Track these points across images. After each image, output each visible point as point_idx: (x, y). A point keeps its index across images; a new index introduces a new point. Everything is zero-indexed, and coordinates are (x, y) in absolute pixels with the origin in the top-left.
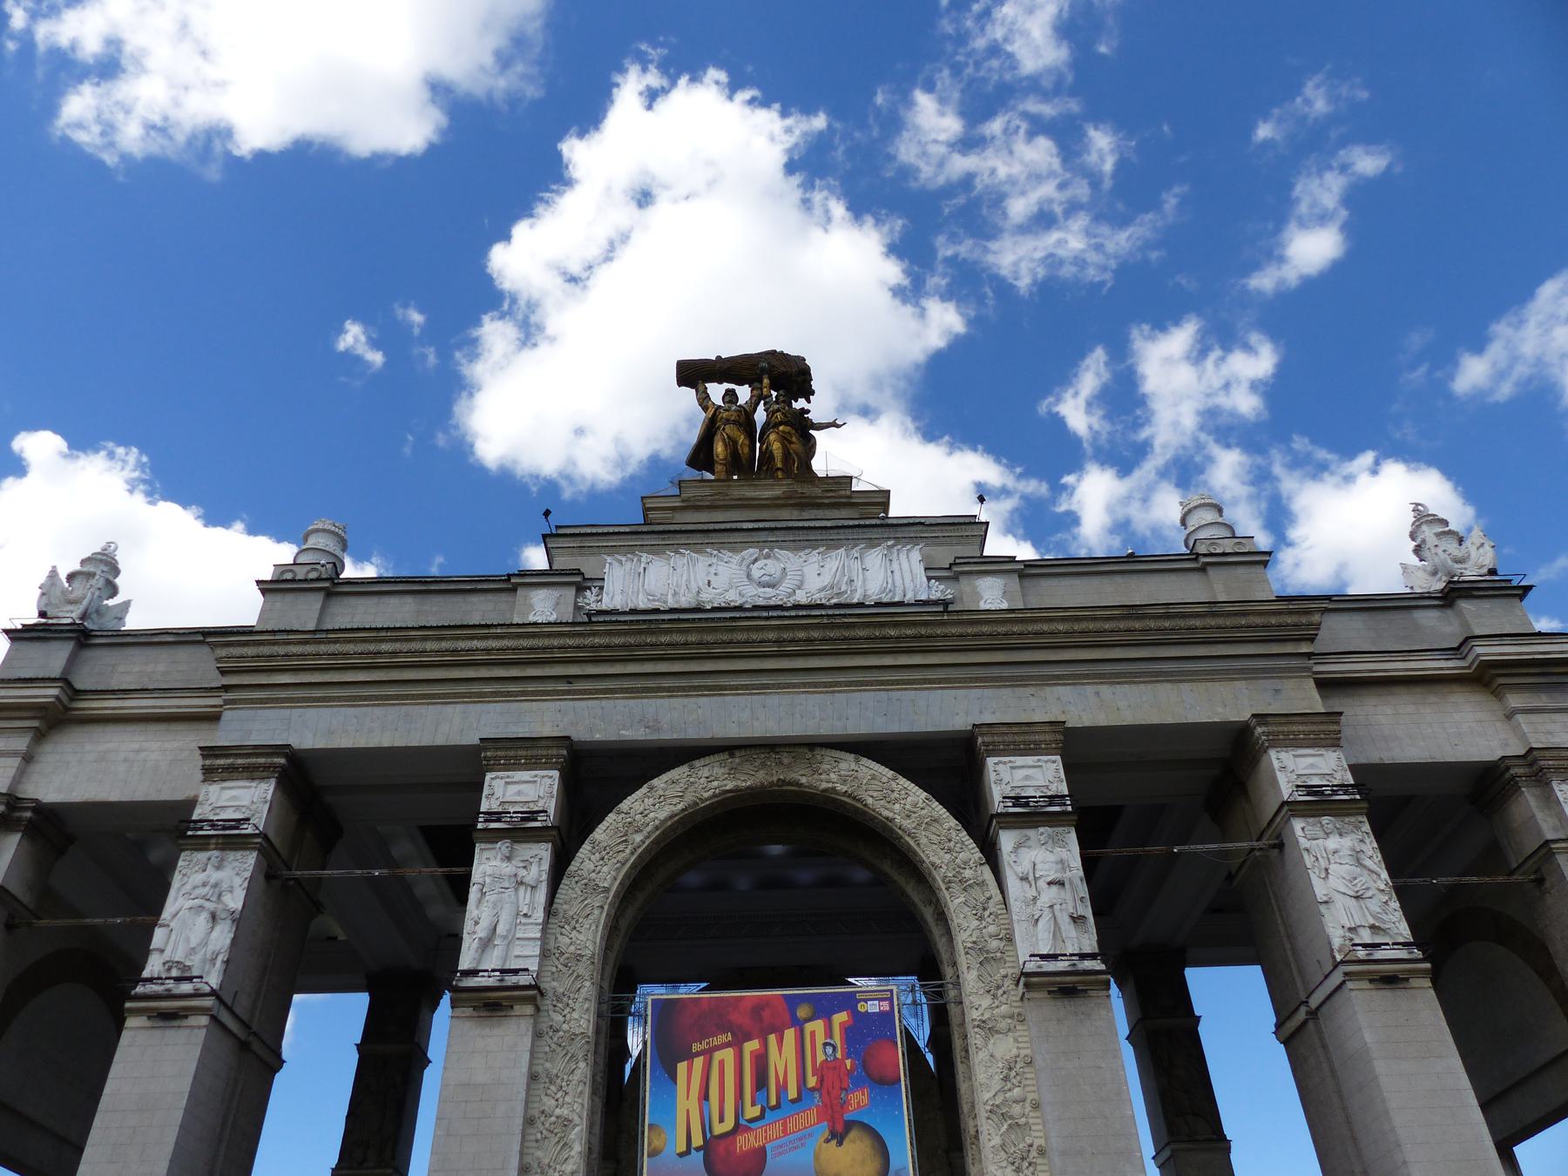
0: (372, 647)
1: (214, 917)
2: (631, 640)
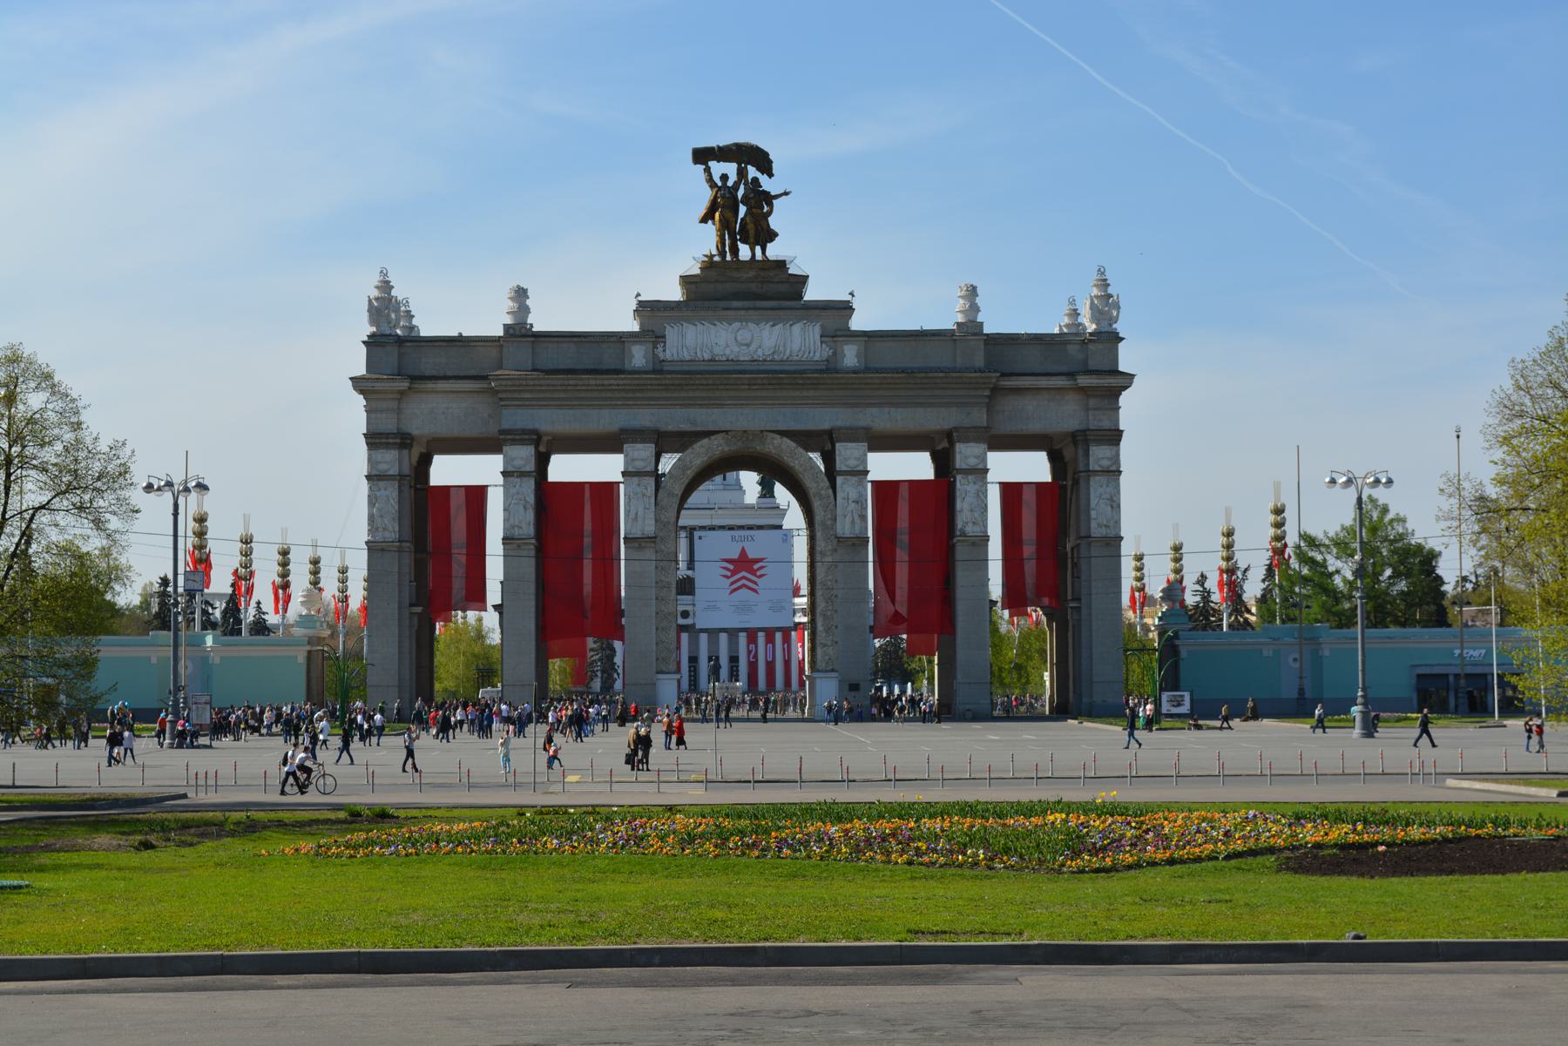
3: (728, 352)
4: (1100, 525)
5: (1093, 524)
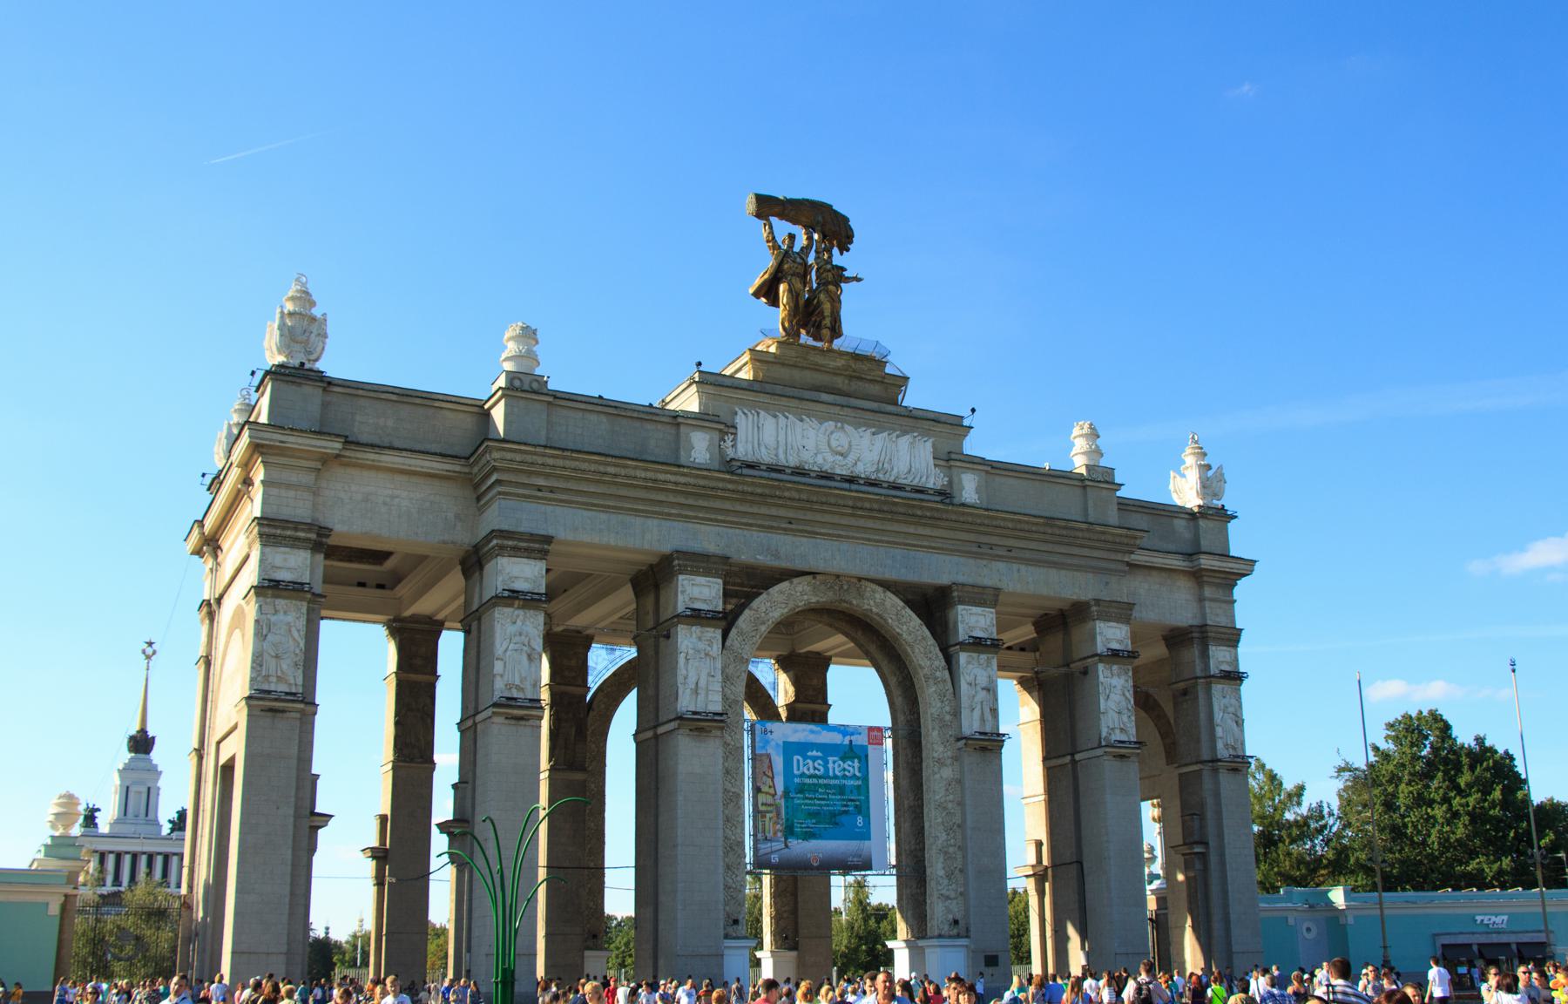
0: (602, 469)
1: (529, 656)
2: (767, 491)
3: (820, 460)
4: (1226, 746)
5: (1220, 745)
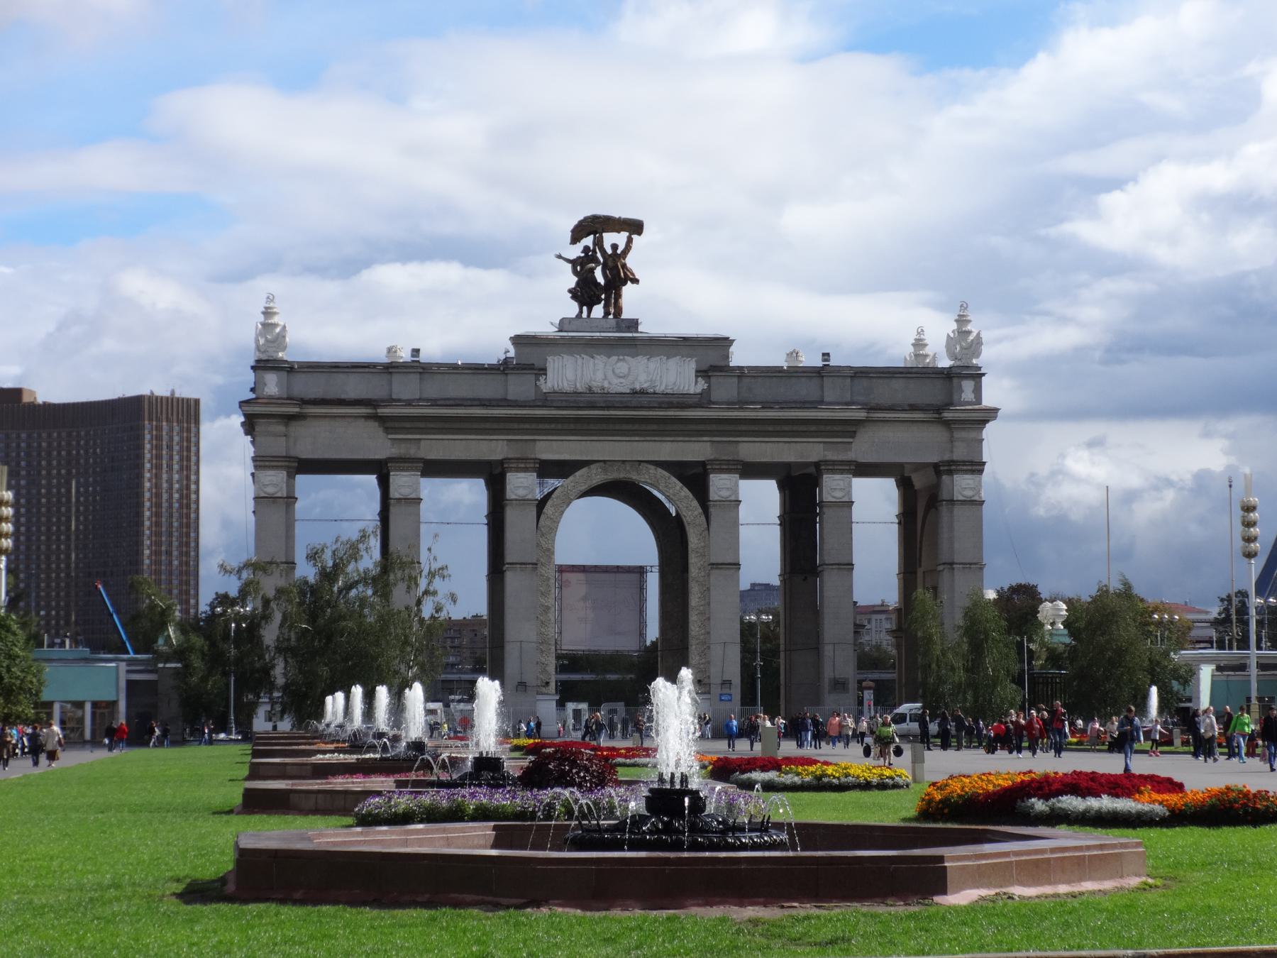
3: (606, 385)
